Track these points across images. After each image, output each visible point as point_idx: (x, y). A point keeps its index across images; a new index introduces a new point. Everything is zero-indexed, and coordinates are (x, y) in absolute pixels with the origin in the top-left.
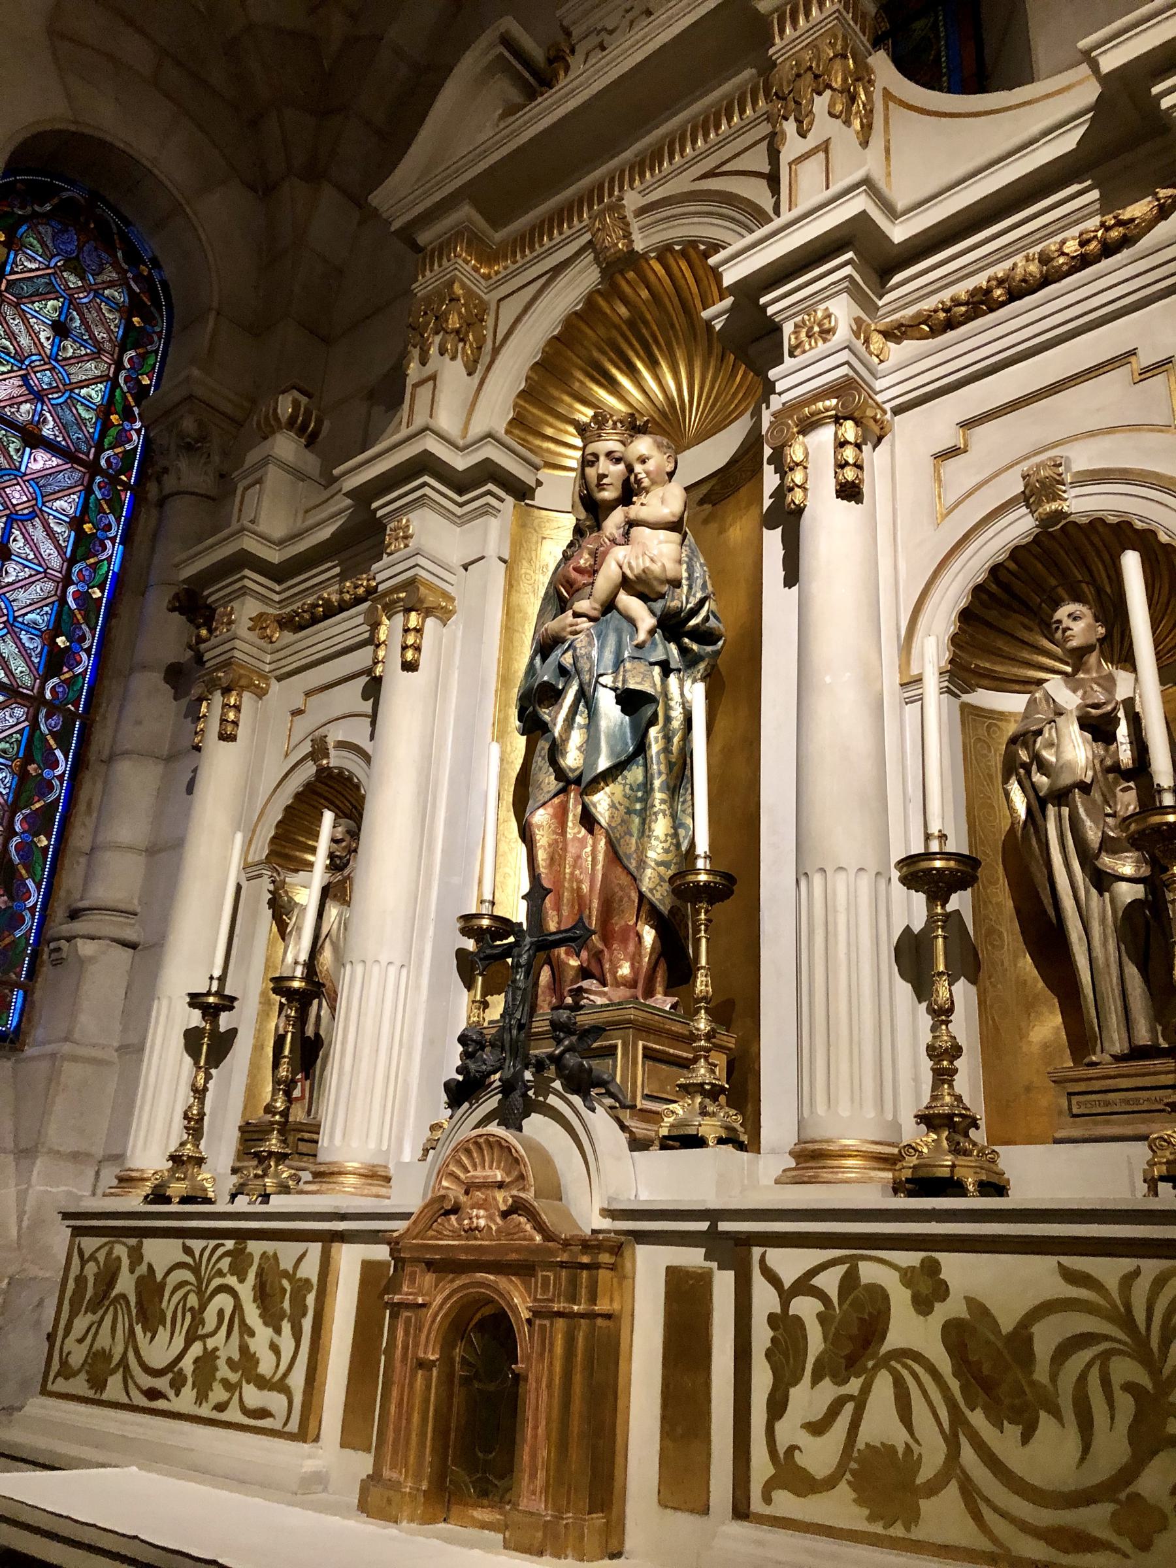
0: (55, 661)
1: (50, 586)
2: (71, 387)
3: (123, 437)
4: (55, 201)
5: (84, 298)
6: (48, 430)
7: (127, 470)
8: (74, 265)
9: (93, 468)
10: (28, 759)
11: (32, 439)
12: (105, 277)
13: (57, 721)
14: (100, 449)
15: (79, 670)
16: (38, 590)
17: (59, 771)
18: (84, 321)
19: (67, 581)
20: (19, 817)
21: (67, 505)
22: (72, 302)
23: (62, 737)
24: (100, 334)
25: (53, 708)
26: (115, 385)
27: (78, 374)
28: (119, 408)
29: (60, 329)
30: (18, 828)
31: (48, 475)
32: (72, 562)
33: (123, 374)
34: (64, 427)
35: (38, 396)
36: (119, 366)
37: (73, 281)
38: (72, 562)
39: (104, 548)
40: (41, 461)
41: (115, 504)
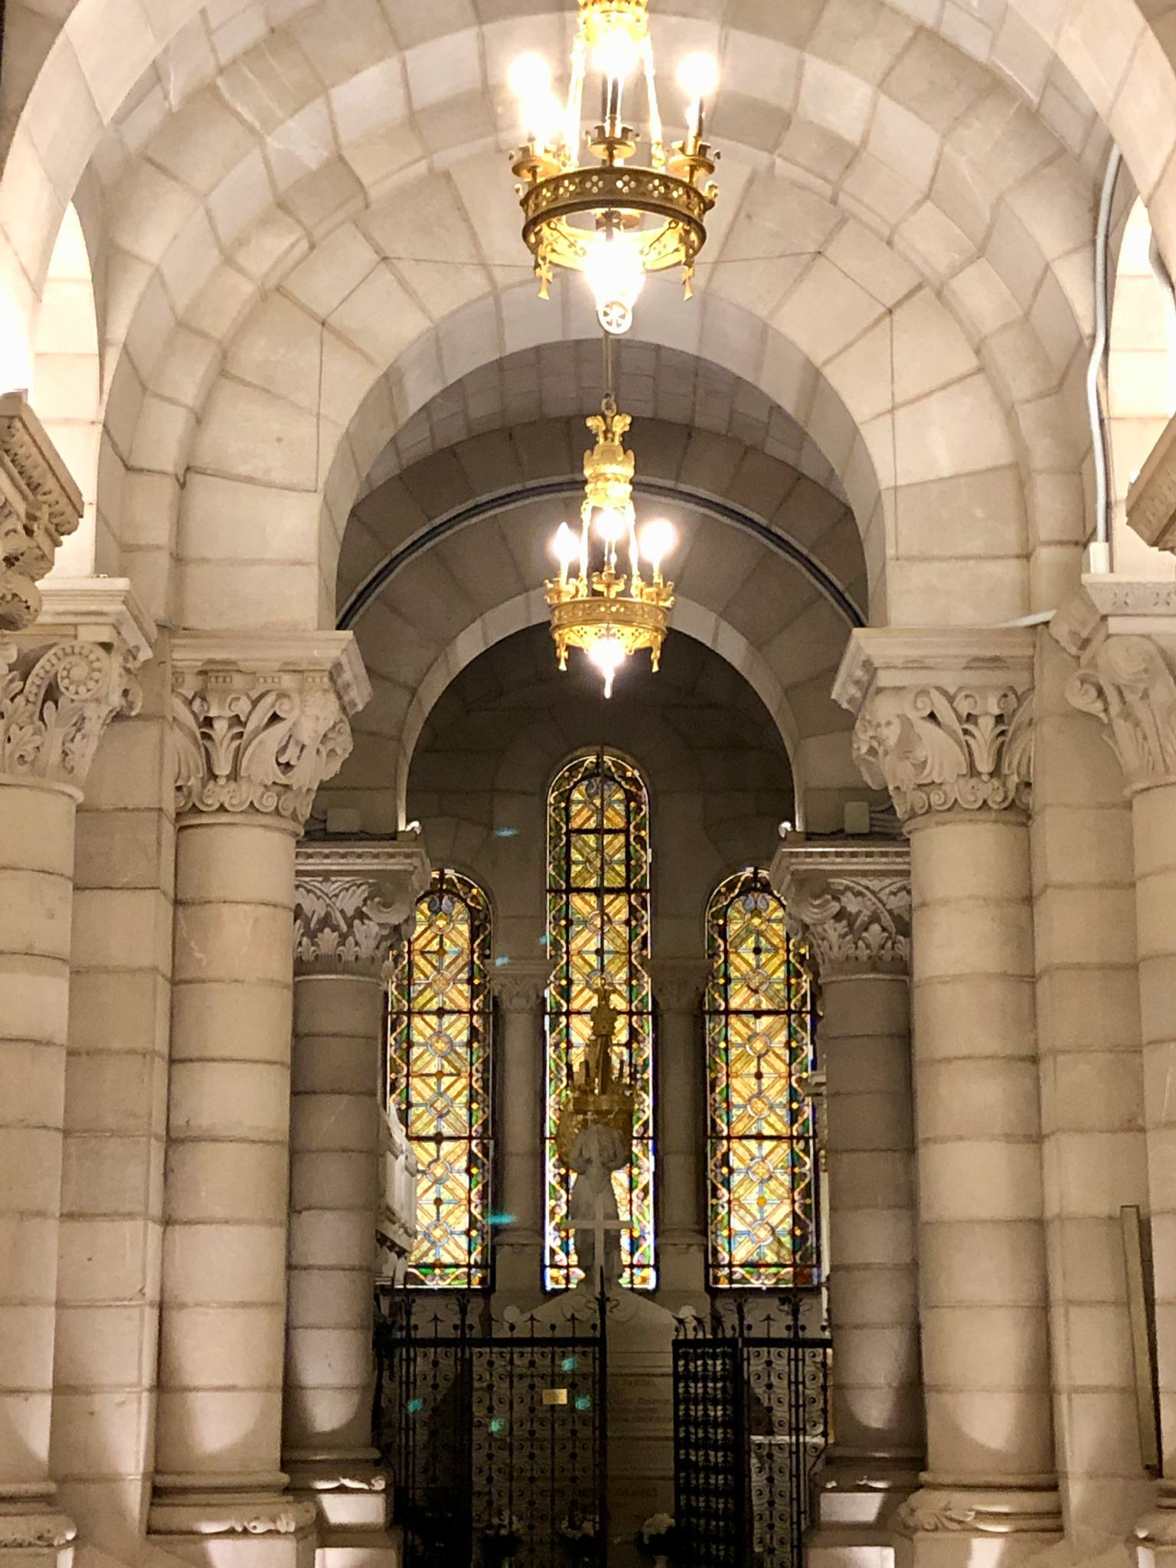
0: (794, 1116)
1: (783, 1081)
2: (769, 977)
3: (799, 986)
4: (739, 885)
5: (763, 927)
6: (765, 1006)
7: (804, 1003)
8: (756, 912)
9: (789, 1012)
10: (793, 1166)
11: (758, 1014)
12: (771, 908)
13: (802, 1144)
14: (789, 1000)
15: (805, 1116)
16: (778, 1086)
17: (807, 1167)
18: (767, 940)
19: (790, 1075)
20: (796, 1193)
21: (782, 1037)
22: (759, 933)
23: (806, 1151)
24: (776, 941)
25: (799, 1138)
26: (788, 962)
27: (769, 969)
28: (792, 974)
29: (757, 951)
30: (797, 1197)
31: (770, 1027)
32: (790, 1065)
33: (791, 954)
34: (771, 999)
35: (756, 991)
36: (788, 951)
37: (756, 921)
38: (790, 1065)
39: (803, 1050)
40: (766, 1021)
41: (803, 1025)
